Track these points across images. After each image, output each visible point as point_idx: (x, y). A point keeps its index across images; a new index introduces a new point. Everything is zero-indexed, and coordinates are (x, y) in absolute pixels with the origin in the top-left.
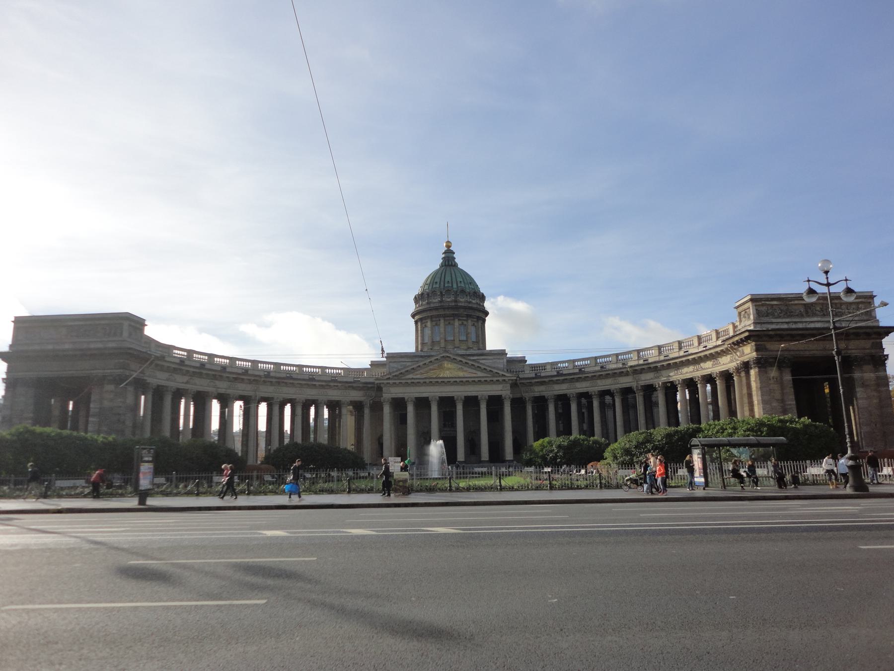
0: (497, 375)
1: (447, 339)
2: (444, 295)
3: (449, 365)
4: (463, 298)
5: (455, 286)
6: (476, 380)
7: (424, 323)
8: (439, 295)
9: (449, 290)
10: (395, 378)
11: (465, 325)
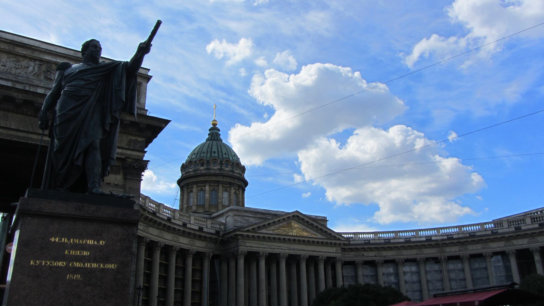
0: (333, 238)
1: (223, 204)
2: (224, 164)
3: (296, 225)
4: (237, 170)
5: (231, 159)
6: (320, 241)
7: (200, 187)
8: (219, 163)
9: (228, 161)
10: (253, 231)
11: (237, 194)
